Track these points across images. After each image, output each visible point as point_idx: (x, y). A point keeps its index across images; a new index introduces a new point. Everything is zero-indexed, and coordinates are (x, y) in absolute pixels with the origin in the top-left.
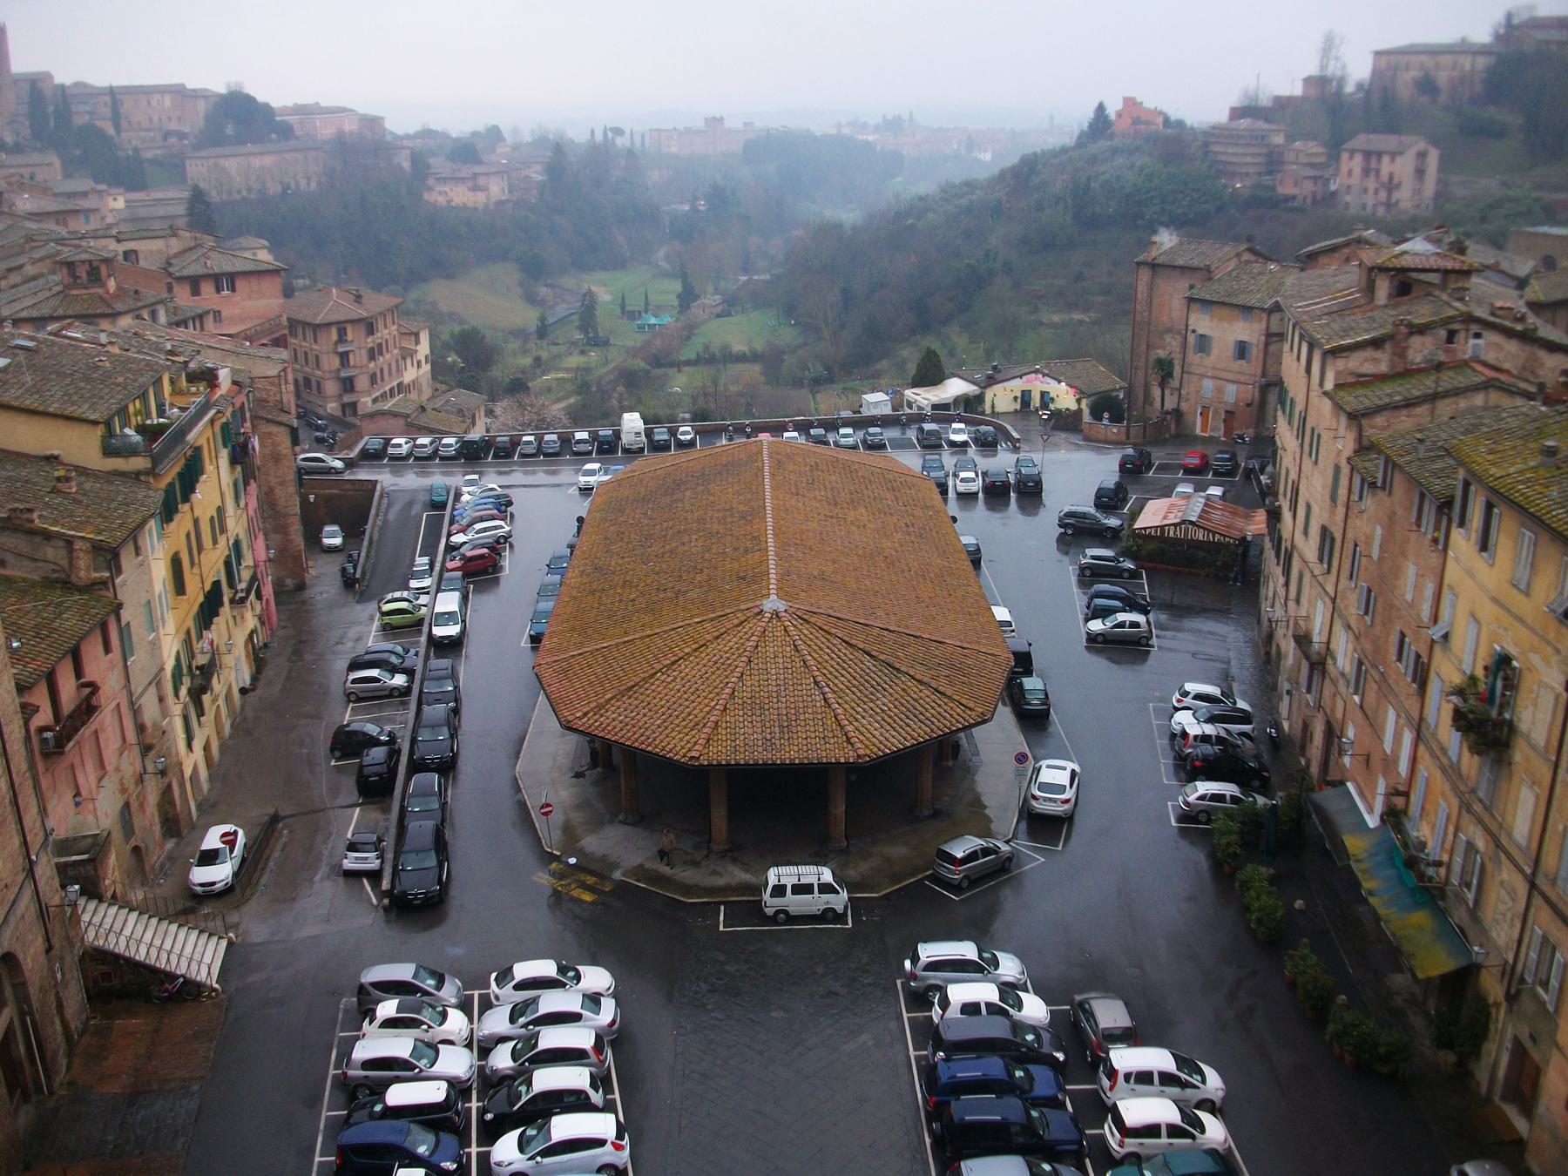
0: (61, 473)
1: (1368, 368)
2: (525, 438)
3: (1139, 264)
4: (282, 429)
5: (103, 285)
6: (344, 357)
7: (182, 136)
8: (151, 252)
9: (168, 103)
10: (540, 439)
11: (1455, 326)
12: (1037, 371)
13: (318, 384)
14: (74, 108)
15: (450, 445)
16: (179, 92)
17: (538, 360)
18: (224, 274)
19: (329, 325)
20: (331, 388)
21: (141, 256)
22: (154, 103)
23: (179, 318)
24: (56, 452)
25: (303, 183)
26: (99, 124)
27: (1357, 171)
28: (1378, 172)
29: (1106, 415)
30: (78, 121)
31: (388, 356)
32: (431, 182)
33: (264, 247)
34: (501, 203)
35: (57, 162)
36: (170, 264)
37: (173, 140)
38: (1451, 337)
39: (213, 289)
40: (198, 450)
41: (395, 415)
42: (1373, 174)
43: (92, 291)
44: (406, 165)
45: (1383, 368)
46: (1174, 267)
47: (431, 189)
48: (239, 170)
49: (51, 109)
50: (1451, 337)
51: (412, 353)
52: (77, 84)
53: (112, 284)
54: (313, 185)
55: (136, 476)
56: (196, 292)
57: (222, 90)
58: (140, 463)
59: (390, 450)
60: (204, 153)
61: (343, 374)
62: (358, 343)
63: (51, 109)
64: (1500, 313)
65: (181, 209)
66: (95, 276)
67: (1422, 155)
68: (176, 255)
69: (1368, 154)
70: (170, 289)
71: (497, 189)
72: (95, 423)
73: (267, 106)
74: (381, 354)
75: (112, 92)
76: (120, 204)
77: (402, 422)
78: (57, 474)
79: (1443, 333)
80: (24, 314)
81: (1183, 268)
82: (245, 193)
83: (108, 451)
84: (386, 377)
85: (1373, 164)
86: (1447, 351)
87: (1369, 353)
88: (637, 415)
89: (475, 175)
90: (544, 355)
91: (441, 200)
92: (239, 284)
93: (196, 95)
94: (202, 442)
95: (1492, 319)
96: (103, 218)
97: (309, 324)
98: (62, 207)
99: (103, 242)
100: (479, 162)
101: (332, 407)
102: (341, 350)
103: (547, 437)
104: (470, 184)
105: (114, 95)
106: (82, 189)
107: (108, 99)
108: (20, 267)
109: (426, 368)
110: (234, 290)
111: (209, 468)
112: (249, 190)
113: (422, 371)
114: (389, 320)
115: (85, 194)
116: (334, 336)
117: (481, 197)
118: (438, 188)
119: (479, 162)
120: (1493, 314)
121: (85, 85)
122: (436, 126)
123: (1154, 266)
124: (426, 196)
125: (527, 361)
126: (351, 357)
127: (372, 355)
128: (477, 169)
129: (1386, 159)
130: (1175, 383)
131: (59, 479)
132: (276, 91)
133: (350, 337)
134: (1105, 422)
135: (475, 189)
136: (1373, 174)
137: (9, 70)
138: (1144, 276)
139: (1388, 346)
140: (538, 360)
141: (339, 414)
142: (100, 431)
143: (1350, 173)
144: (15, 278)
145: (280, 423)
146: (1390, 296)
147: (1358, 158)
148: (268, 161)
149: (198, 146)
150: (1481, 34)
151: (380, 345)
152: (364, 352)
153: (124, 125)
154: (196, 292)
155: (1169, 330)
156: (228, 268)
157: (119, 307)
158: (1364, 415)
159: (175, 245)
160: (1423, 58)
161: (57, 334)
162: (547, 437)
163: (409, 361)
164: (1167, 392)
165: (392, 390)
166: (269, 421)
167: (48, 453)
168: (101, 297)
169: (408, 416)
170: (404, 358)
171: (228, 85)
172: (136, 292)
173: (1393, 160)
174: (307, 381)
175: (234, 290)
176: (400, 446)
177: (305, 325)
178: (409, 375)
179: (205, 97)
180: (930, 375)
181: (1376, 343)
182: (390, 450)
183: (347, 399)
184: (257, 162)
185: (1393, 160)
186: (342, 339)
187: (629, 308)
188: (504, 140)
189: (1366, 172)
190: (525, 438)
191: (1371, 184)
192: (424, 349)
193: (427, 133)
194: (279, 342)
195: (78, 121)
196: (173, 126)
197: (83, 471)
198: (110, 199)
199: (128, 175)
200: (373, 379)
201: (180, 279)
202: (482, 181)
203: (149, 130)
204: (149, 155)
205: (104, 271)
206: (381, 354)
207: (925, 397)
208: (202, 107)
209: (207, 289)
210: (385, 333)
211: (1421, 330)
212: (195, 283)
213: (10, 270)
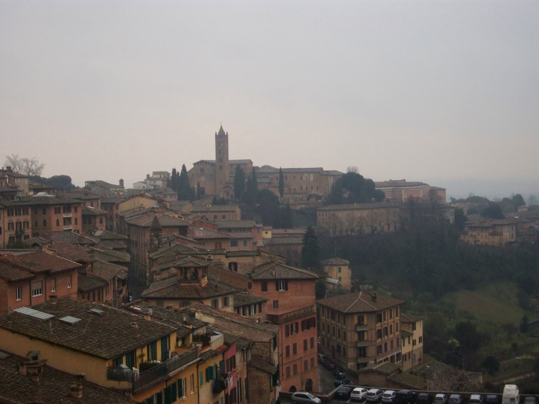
2: (438, 396)
4: (264, 375)
5: (199, 281)
6: (361, 334)
7: (318, 197)
8: (245, 265)
10: (447, 395)
14: (259, 180)
15: (390, 395)
16: (319, 172)
17: (515, 346)
18: (282, 279)
19: (353, 314)
20: (351, 353)
21: (239, 266)
23: (245, 303)
24: (83, 374)
25: (386, 228)
26: (270, 189)
30: (260, 188)
31: (391, 336)
32: (466, 229)
33: (346, 265)
34: (511, 243)
35: (238, 211)
37: (313, 200)
39: (274, 288)
43: (192, 284)
44: (452, 219)
47: (466, 234)
48: (349, 217)
49: (246, 180)
51: (410, 335)
52: (264, 167)
53: (205, 281)
54: (392, 229)
55: (123, 392)
56: (264, 289)
57: (345, 171)
58: (125, 385)
59: (352, 395)
60: (327, 208)
61: (359, 345)
62: (371, 327)
63: (246, 180)
65: (300, 240)
66: (196, 278)
68: (259, 267)
70: (250, 286)
71: (507, 235)
72: (105, 359)
73: (370, 181)
74: (387, 334)
75: (281, 172)
76: (269, 235)
77: (384, 378)
78: (72, 386)
80: (152, 295)
82: (350, 233)
83: (111, 376)
88: (514, 387)
89: (494, 226)
90: (520, 343)
91: (471, 240)
92: (290, 286)
93: (329, 174)
96: (255, 243)
97: (341, 313)
98: (220, 236)
99: (218, 257)
100: (502, 217)
101: (351, 365)
102: (359, 330)
103: (452, 396)
104: (491, 231)
105: (282, 174)
106: (248, 226)
107: (278, 175)
108: (168, 269)
110: (286, 289)
112: (352, 230)
113: (415, 347)
114: (394, 314)
115: (250, 229)
116: (356, 321)
117: (496, 240)
118: (470, 233)
119: (502, 217)
121: (269, 167)
122: (479, 193)
124: (462, 237)
125: (508, 346)
126: (365, 334)
127: (379, 334)
128: (496, 222)
131: (73, 389)
132: (375, 172)
133: (365, 322)
135: (494, 234)
137: (228, 158)
140: (515, 346)
141: (355, 370)
144: (165, 275)
145: (264, 371)
148: (365, 213)
149: (325, 204)
151: (386, 328)
152: (374, 332)
153: (286, 189)
154: (264, 289)
156: (284, 276)
157: (204, 294)
159: (259, 261)
162: (452, 396)
163: (406, 340)
165: (392, 357)
166: (257, 369)
167: (79, 374)
168: (196, 289)
169: (388, 375)
170: (403, 338)
171: (349, 168)
172: (216, 287)
174: (339, 346)
175: (286, 289)
176: (358, 392)
177: (340, 313)
178: (406, 349)
179: (334, 175)
182: (352, 395)
183: (360, 361)
184: (358, 214)
188: (524, 203)
190: (438, 396)
192: (418, 332)
193: (473, 199)
194: (308, 324)
195: (260, 188)
196: (314, 192)
197: (94, 386)
198: (264, 232)
199: (280, 218)
200: (379, 349)
201: (256, 281)
202: (498, 229)
203: (299, 194)
204: (298, 208)
205: (200, 273)
206: (387, 334)
208: (331, 181)
209: (271, 287)
210: (392, 320)
212: (264, 284)
213: (162, 270)
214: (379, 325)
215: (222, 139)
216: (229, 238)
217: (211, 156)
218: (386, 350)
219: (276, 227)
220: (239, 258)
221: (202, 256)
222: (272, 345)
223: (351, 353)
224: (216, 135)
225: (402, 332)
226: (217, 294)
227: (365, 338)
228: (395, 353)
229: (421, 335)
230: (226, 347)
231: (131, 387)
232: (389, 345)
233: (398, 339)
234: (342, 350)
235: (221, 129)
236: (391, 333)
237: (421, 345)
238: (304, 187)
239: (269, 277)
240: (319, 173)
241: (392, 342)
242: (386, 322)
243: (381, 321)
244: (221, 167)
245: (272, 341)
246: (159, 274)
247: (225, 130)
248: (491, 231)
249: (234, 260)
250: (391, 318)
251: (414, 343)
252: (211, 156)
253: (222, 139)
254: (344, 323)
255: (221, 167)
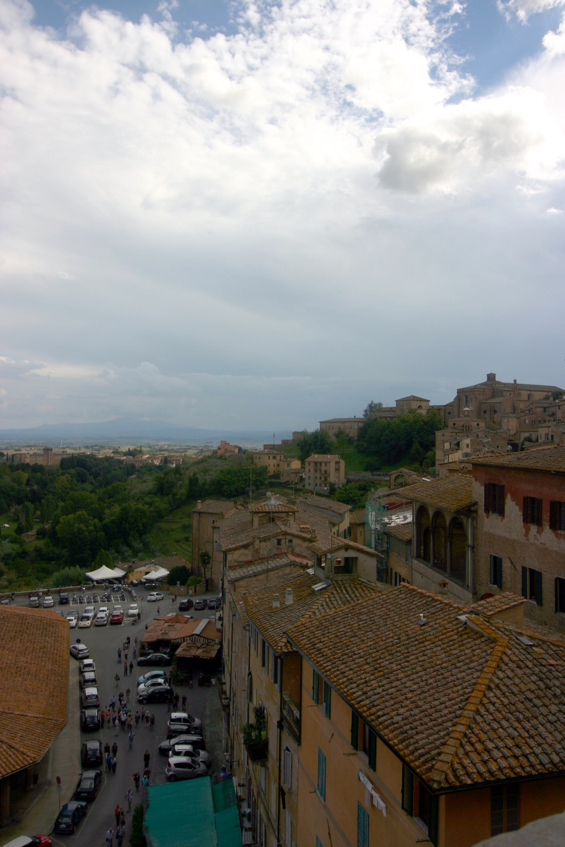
1: (243, 559)
3: (194, 512)
11: (280, 537)
12: (152, 563)
27: (312, 470)
28: (321, 470)
29: (178, 582)
38: (279, 542)
42: (318, 471)
45: (249, 558)
46: (208, 513)
50: (279, 542)
64: (303, 530)
67: (338, 463)
69: (316, 463)
79: (276, 541)
81: (212, 513)
85: (319, 467)
86: (278, 549)
87: (243, 551)
95: (300, 533)
120: (301, 531)
123: (200, 513)
129: (323, 465)
130: (209, 566)
134: (178, 586)
136: (318, 471)
138: (196, 517)
139: (251, 547)
143: (309, 470)
146: (259, 525)
147: (312, 464)
150: (360, 415)
155: (207, 542)
158: (236, 581)
160: (339, 424)
164: (206, 571)
173: (326, 465)
181: (246, 547)
185: (326, 465)
189: (316, 471)
191: (318, 475)
211: (265, 540)
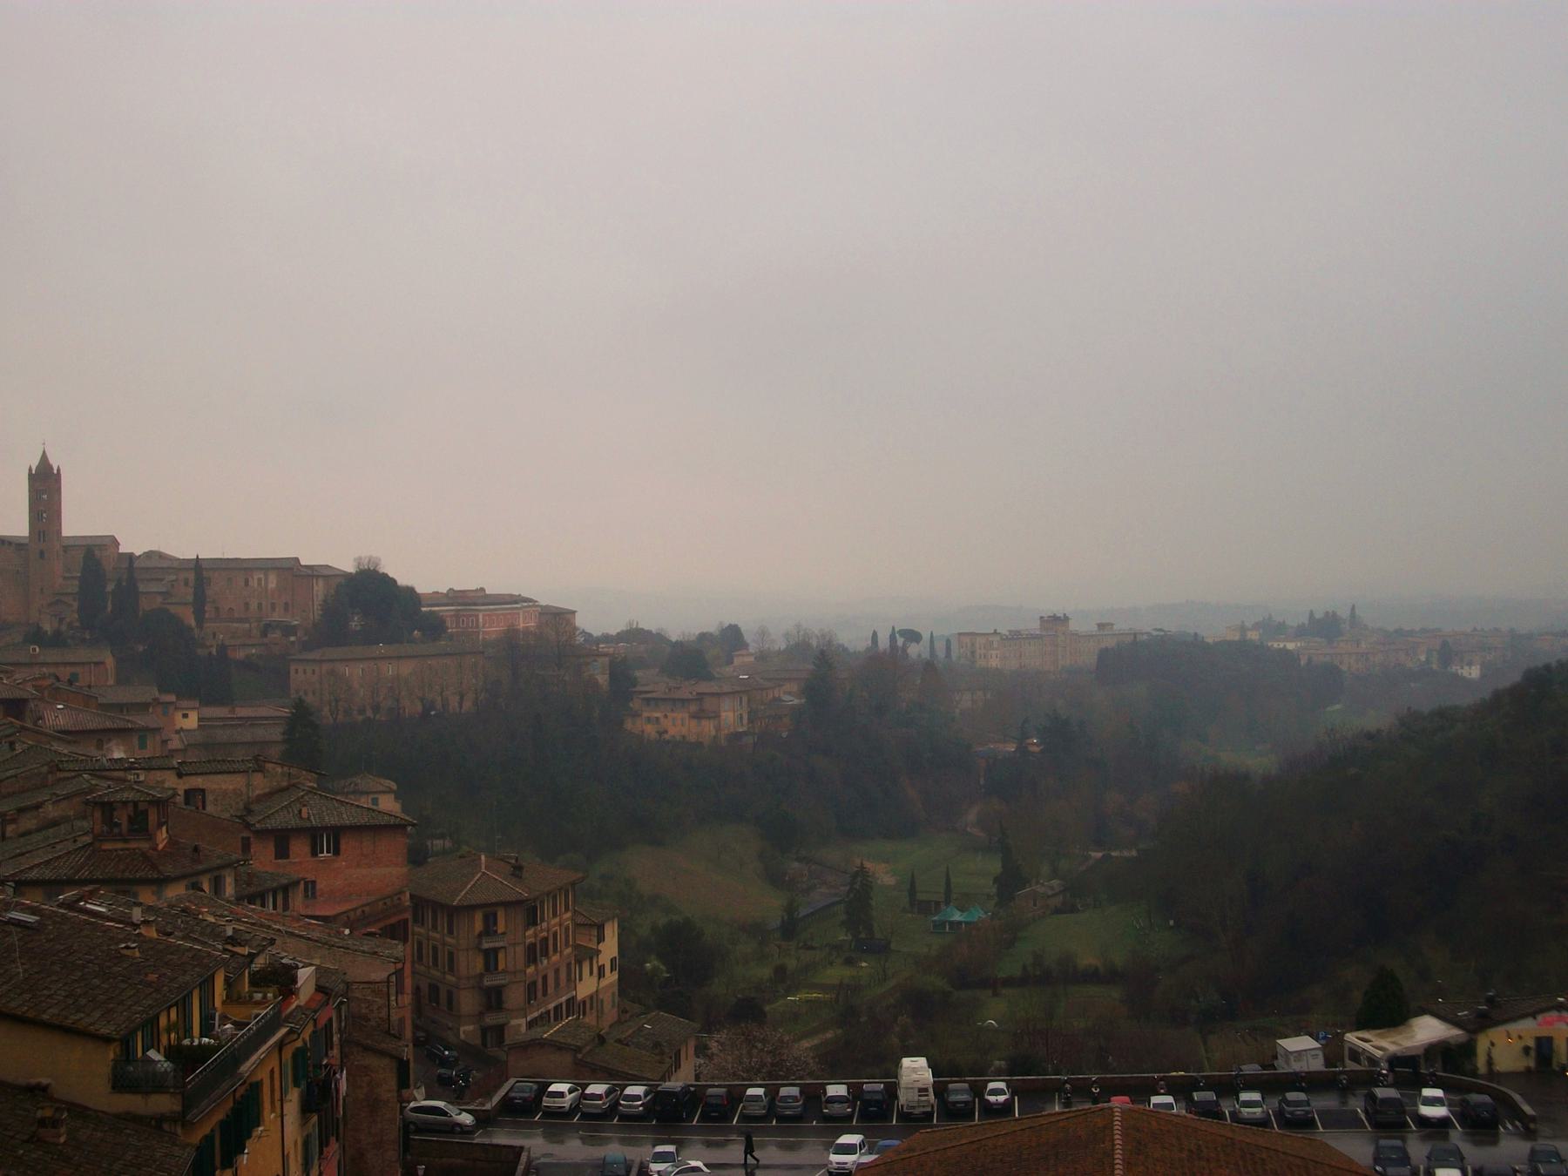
0: (48, 1113)
2: (750, 1091)
4: (386, 1061)
5: (150, 837)
6: (491, 956)
7: (289, 630)
9: (272, 584)
10: (772, 1092)
13: (450, 994)
14: (142, 588)
15: (637, 1098)
16: (291, 569)
17: (780, 971)
18: (325, 828)
19: (472, 908)
20: (468, 1002)
21: (210, 798)
22: (254, 583)
23: (252, 890)
24: (45, 1081)
25: (454, 702)
26: (173, 609)
30: (145, 605)
31: (555, 958)
32: (635, 704)
33: (390, 791)
34: (737, 736)
35: (110, 662)
36: (249, 811)
37: (276, 635)
39: (307, 849)
40: (256, 1087)
41: (559, 1047)
43: (133, 845)
44: (603, 679)
47: (636, 715)
48: (366, 677)
49: (110, 587)
52: (149, 555)
53: (162, 836)
54: (467, 705)
55: (158, 1121)
56: (282, 852)
57: (350, 568)
58: (163, 1103)
59: (546, 1102)
60: (315, 655)
61: (487, 982)
62: (512, 936)
63: (110, 587)
65: (276, 733)
66: (139, 826)
68: (259, 799)
70: (246, 846)
71: (731, 716)
72: (107, 1040)
73: (410, 591)
74: (545, 954)
76: (192, 722)
77: (568, 1058)
78: (39, 1114)
80: (33, 875)
82: (369, 713)
83: (121, 1083)
84: (550, 990)
88: (922, 1062)
89: (701, 697)
90: (791, 964)
91: (650, 730)
92: (346, 844)
94: (263, 1075)
96: (165, 742)
98: (109, 724)
100: (709, 678)
101: (467, 1030)
102: (486, 946)
103: (784, 1091)
104: (693, 708)
105: (200, 570)
107: (192, 576)
108: (38, 807)
109: (612, 977)
110: (337, 852)
111: (269, 1116)
112: (376, 708)
113: (604, 982)
114: (561, 907)
115: (143, 707)
116: (479, 925)
117: (708, 727)
118: (645, 714)
119: (709, 678)
121: (161, 556)
122: (649, 624)
124: (628, 725)
125: (765, 972)
126: (501, 956)
127: (532, 955)
128: (704, 687)
131: (42, 1122)
132: (423, 570)
133: (501, 928)
135: (697, 716)
137: (59, 531)
140: (780, 971)
142: (112, 1053)
144: (28, 822)
145: (382, 1053)
148: (406, 668)
151: (546, 939)
152: (520, 949)
154: (282, 852)
156: (331, 820)
157: (169, 870)
159: (260, 784)
161: (71, 905)
162: (784, 1091)
165: (558, 1008)
166: (366, 1049)
167: (33, 1081)
168: (143, 854)
169: (578, 1050)
170: (580, 962)
171: (359, 561)
172: (196, 849)
174: (434, 989)
175: (337, 852)
176: (561, 1095)
177: (437, 907)
178: (586, 987)
179: (326, 577)
180: (1389, 1011)
182: (546, 1102)
183: (490, 1019)
184: (389, 670)
186: (489, 930)
187: (921, 897)
188: (745, 646)
190: (750, 1091)
192: (609, 948)
193: (634, 635)
194: (396, 932)
195: (145, 605)
196: (276, 617)
197: (79, 1111)
198: (179, 715)
199: (207, 680)
201: (263, 834)
203: (241, 620)
204: (240, 654)
205: (153, 817)
206: (545, 954)
207: (1379, 1044)
208: (319, 588)
209: (300, 848)
210: (555, 922)
212: (281, 841)
213: (21, 811)
214: (530, 932)
215: (45, 485)
216: (131, 730)
217: (17, 525)
218: (545, 993)
219: (208, 701)
220: (211, 777)
221: (116, 774)
222: (393, 990)
223: (468, 1002)
224: (30, 474)
225: (577, 947)
226: (200, 867)
227: (501, 967)
228: (564, 999)
229: (614, 952)
230: (320, 996)
231: (178, 1108)
232: (551, 981)
233: (569, 965)
234: (443, 996)
235: (44, 457)
236: (555, 951)
237: (615, 976)
238: (254, 605)
239: (294, 822)
240: (290, 571)
241: (557, 971)
242: (545, 925)
243: (535, 924)
244: (42, 553)
245: (393, 978)
246: (14, 821)
247: (54, 462)
248: (693, 708)
249: (198, 782)
250: (555, 915)
251: (601, 974)
252: (17, 525)
253: (45, 485)
254: (451, 932)
255: (42, 553)
